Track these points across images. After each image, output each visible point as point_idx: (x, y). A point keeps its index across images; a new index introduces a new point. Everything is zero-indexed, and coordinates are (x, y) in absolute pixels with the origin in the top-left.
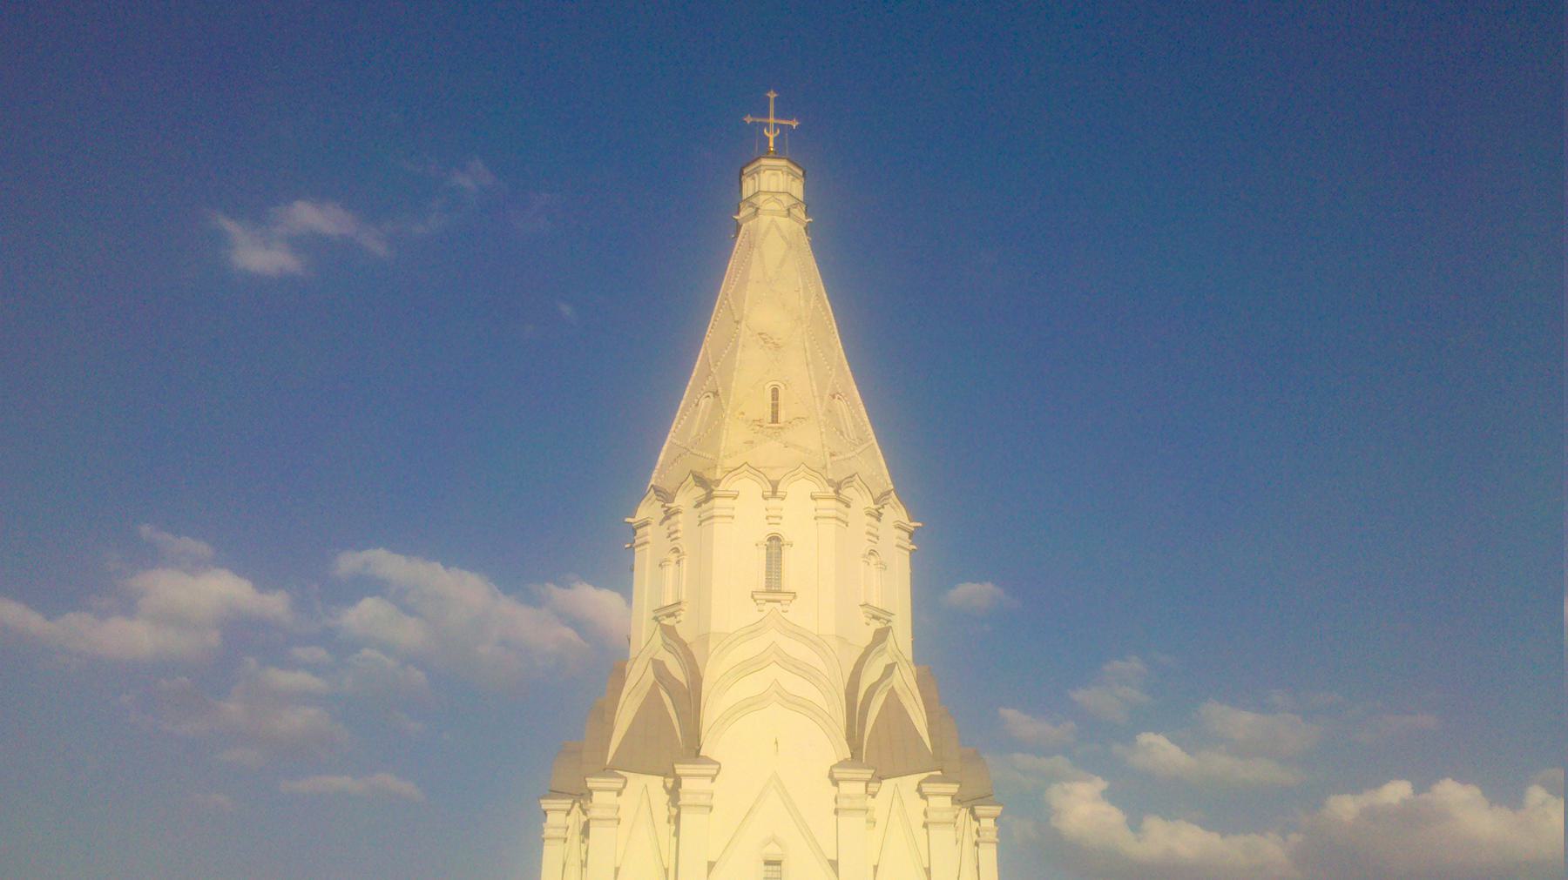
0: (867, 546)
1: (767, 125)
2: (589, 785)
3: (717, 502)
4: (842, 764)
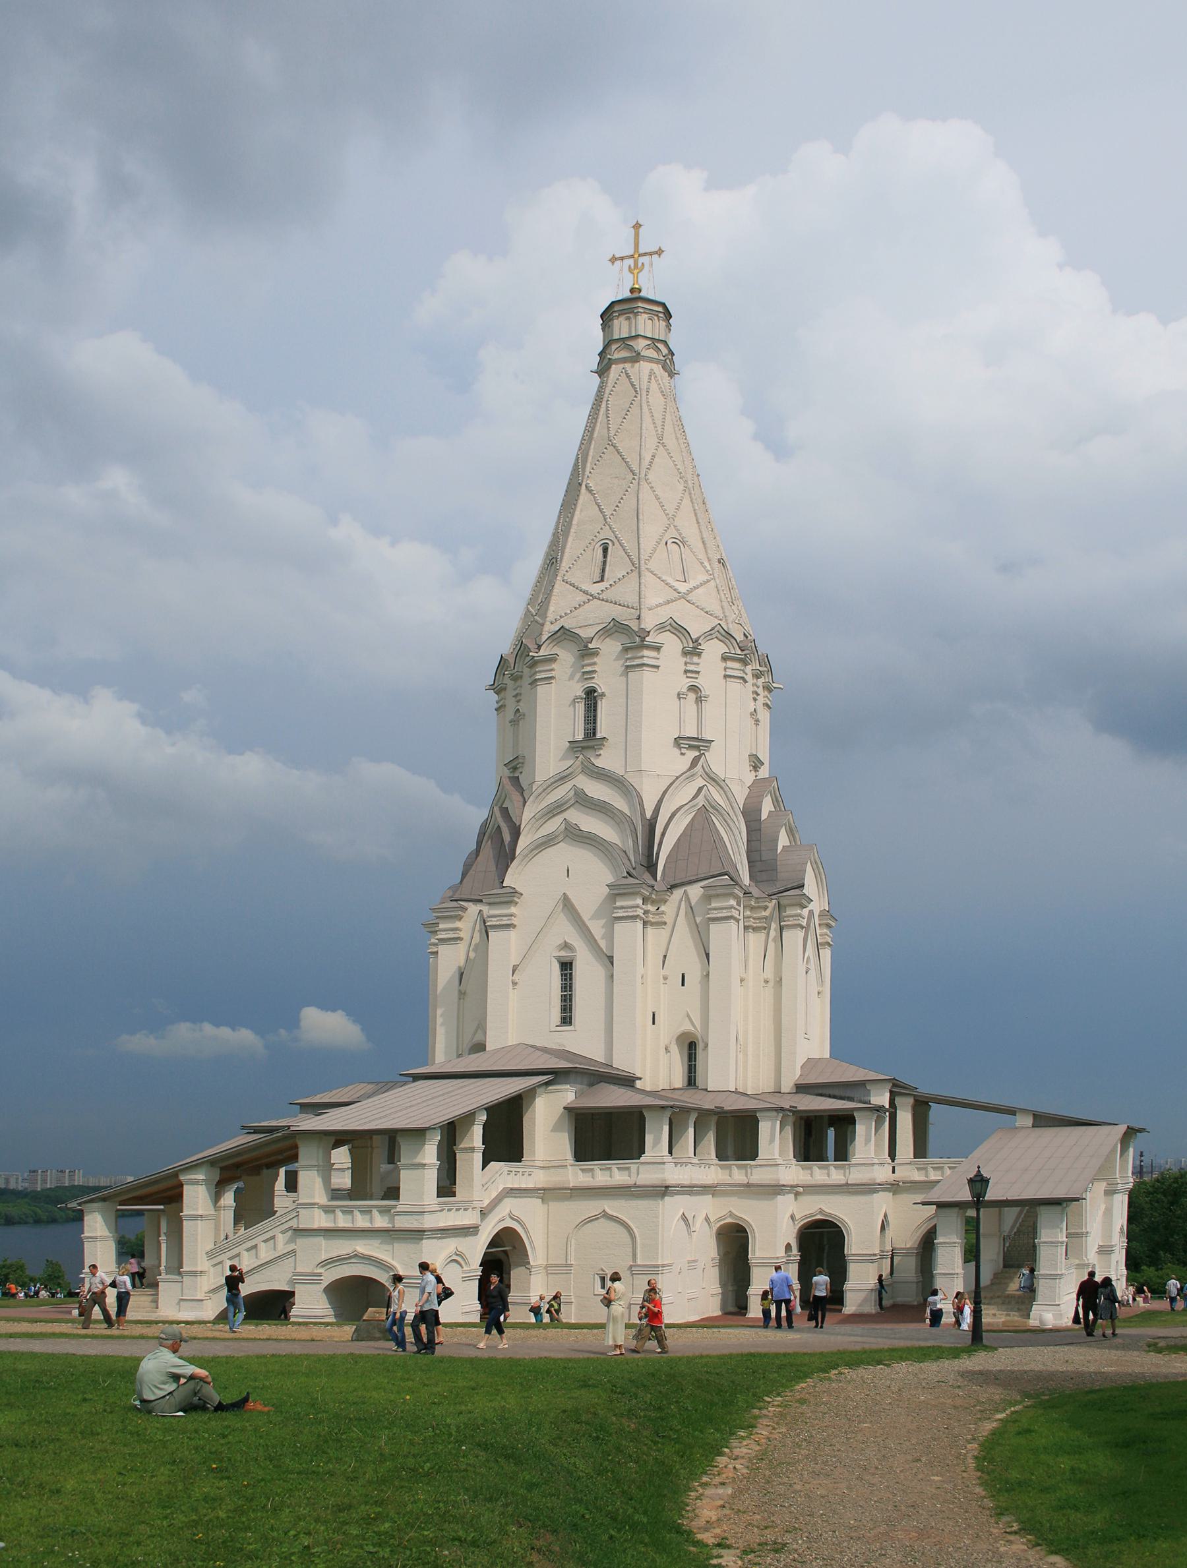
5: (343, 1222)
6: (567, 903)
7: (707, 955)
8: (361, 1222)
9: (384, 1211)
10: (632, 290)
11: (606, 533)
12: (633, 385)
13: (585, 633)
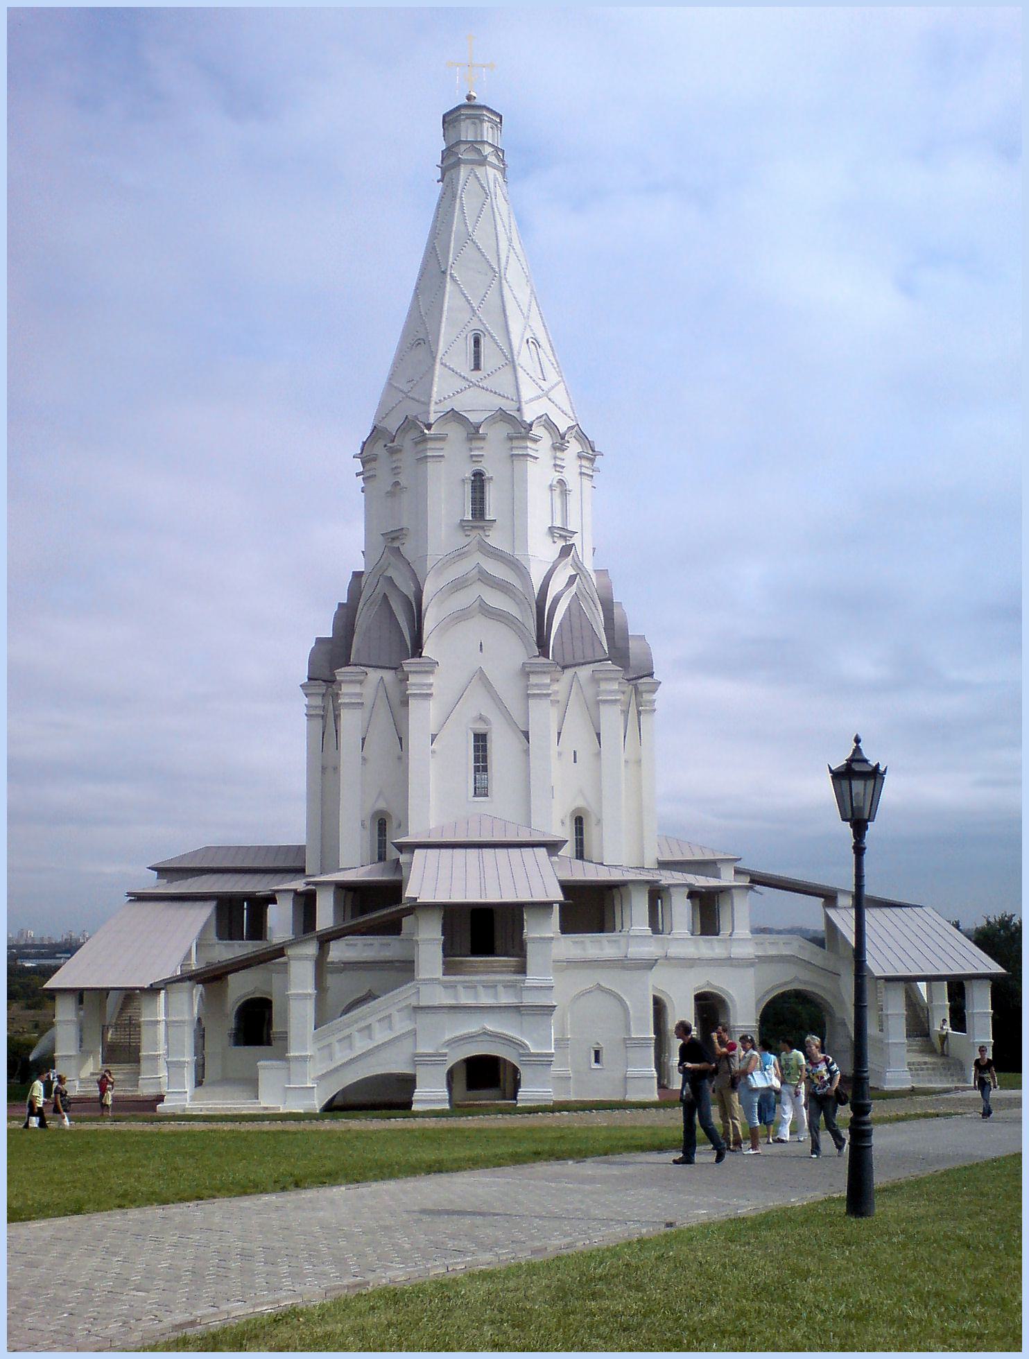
0: (557, 476)
3: (430, 445)
5: (466, 999)
6: (481, 675)
7: (598, 735)
8: (486, 999)
9: (509, 986)
10: (469, 98)
11: (475, 325)
12: (483, 187)
13: (474, 418)
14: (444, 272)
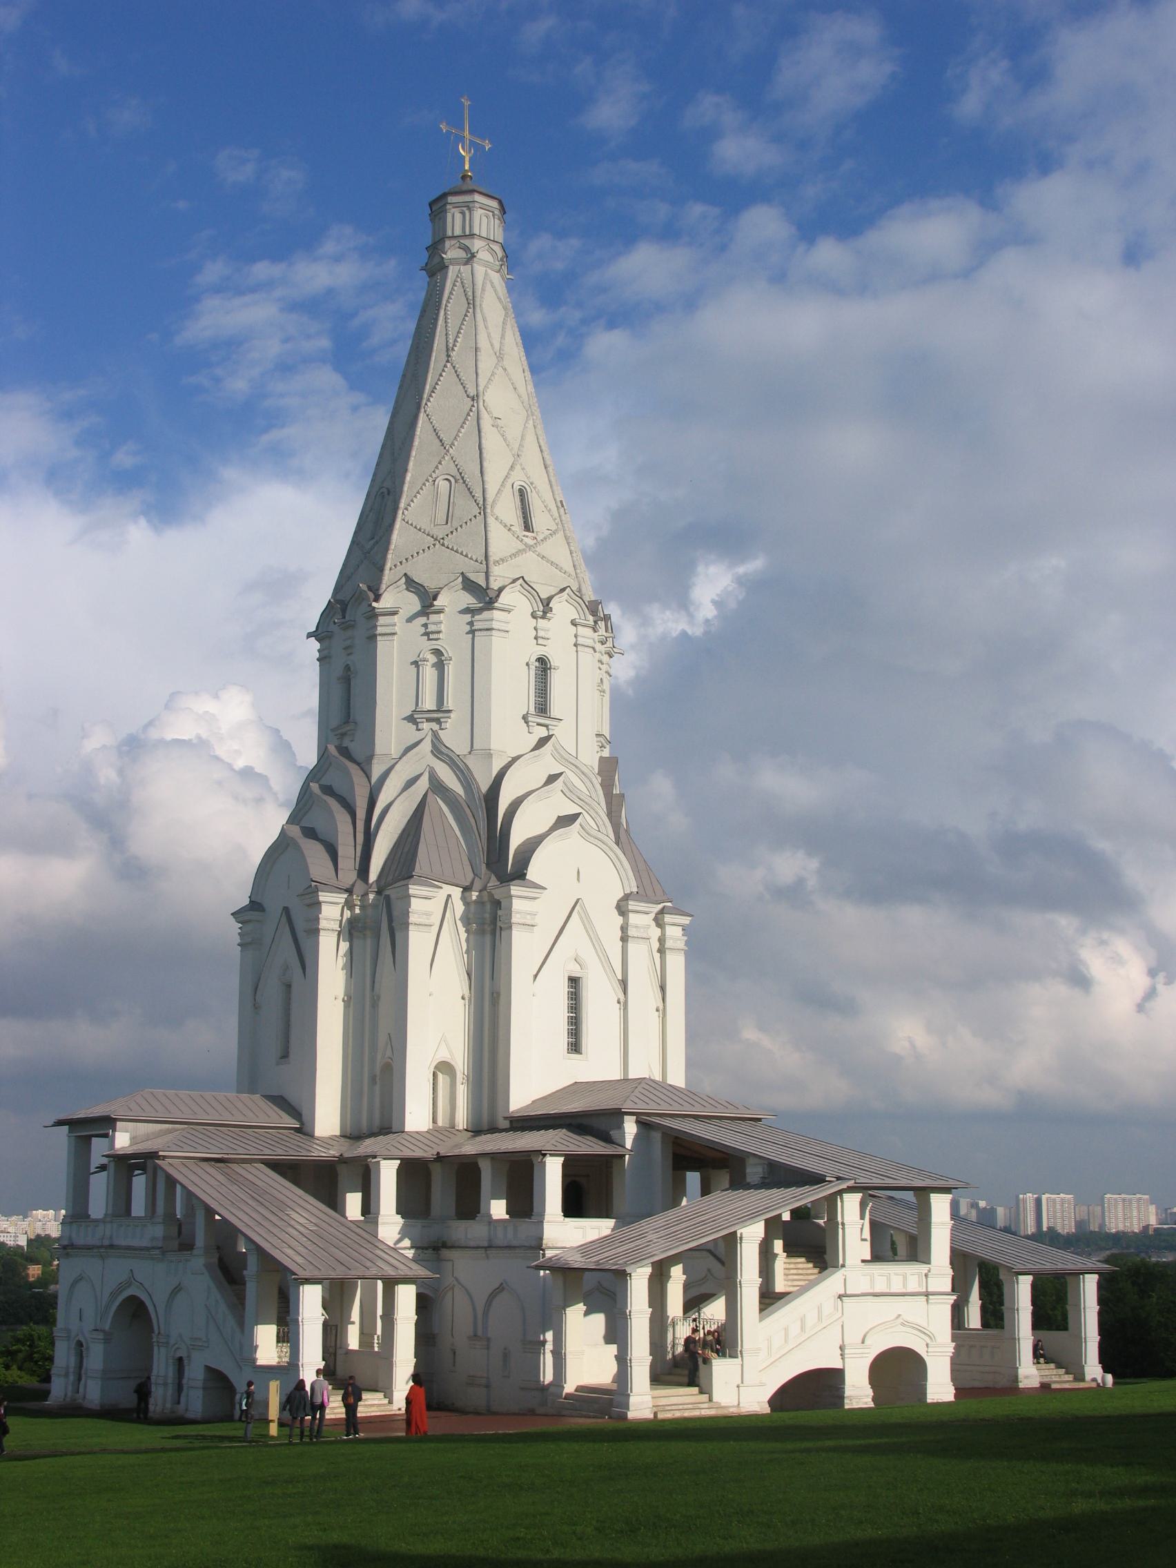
1: (462, 139)
2: (411, 892)
4: (626, 897)
7: (663, 988)
14: (474, 399)
